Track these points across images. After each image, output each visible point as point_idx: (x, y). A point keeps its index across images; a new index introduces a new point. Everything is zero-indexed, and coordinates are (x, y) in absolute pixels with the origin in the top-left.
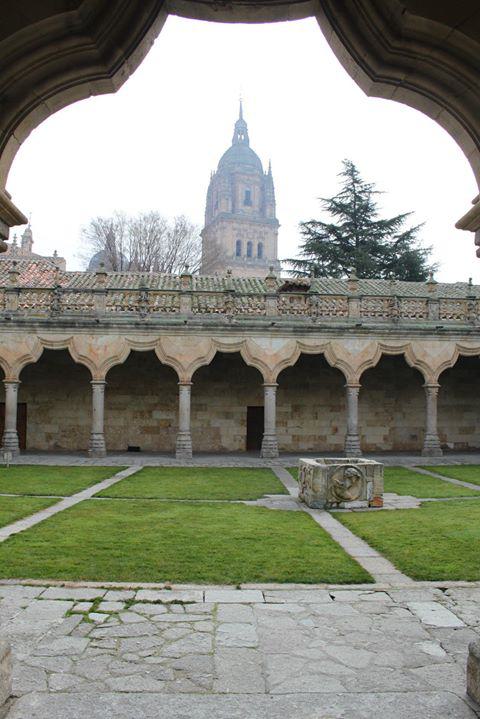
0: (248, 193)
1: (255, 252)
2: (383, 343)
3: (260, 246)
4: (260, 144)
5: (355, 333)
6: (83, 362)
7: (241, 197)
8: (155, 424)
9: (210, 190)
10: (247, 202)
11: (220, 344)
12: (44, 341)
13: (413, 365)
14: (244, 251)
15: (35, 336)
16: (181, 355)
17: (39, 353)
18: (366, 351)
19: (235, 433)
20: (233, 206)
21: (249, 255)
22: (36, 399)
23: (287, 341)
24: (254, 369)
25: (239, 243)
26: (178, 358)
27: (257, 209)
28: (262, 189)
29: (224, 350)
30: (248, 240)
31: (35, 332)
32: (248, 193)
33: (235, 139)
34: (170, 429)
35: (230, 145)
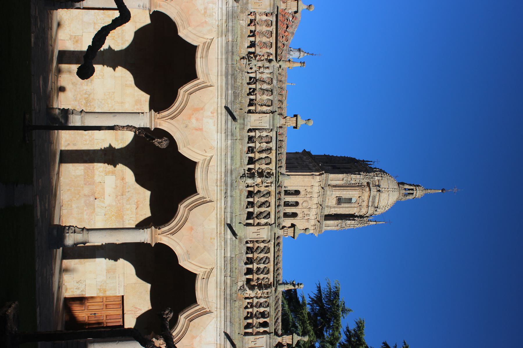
7: (345, 194)
8: (97, 179)
12: (208, 46)
15: (214, 35)
19: (88, 282)
21: (287, 204)
25: (297, 193)
27: (333, 211)
29: (199, 284)
31: (221, 34)
32: (349, 201)
34: (92, 199)
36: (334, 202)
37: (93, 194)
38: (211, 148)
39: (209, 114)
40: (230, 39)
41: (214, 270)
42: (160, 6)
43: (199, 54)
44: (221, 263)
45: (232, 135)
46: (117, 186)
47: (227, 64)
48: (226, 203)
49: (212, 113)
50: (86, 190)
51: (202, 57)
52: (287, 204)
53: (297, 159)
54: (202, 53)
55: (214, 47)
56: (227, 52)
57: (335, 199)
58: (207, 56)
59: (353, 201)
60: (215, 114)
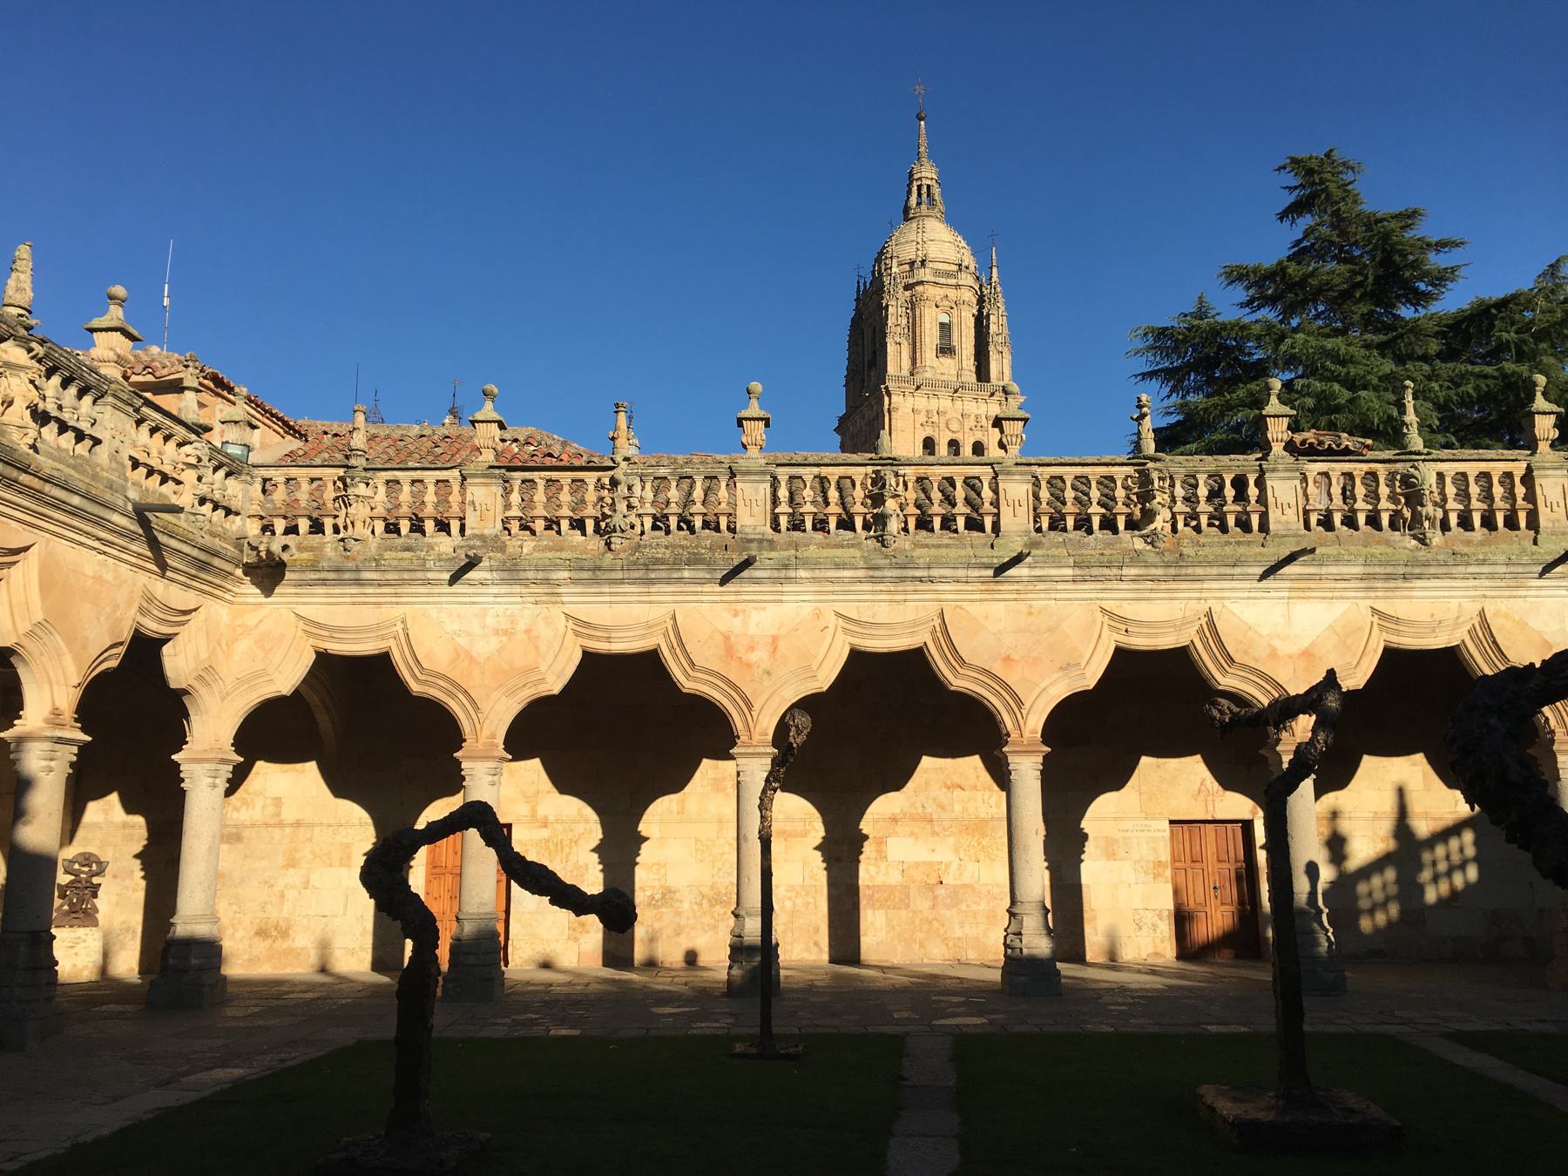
7: (931, 337)
8: (895, 878)
15: (556, 612)
16: (1007, 659)
19: (1137, 904)
22: (540, 812)
23: (1340, 607)
27: (969, 363)
30: (950, 436)
32: (945, 329)
34: (941, 891)
36: (948, 363)
37: (931, 888)
39: (738, 621)
40: (566, 574)
41: (1107, 605)
42: (493, 736)
44: (1088, 590)
45: (786, 567)
46: (912, 834)
47: (621, 581)
48: (943, 580)
49: (736, 615)
50: (922, 904)
51: (608, 640)
54: (598, 639)
55: (584, 612)
56: (595, 581)
58: (605, 628)
59: (945, 319)
60: (739, 606)
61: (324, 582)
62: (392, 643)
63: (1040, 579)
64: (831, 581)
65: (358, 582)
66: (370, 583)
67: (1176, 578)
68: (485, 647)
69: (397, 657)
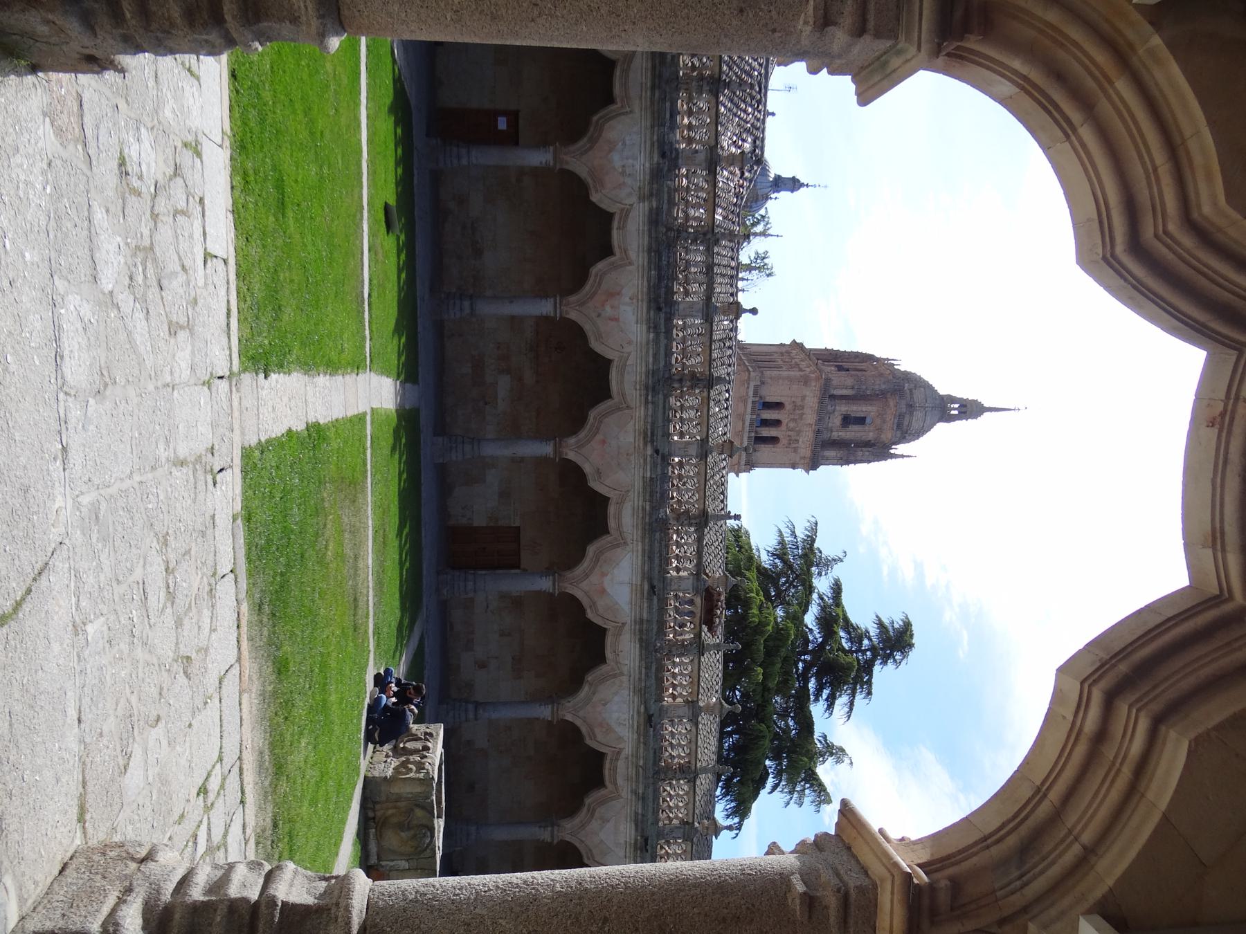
0: (861, 421)
1: (766, 432)
2: (623, 755)
3: (774, 440)
4: (942, 437)
5: (639, 712)
6: (591, 280)
7: (856, 409)
9: (870, 358)
10: (847, 420)
11: (621, 503)
12: (626, 213)
13: (588, 801)
14: (767, 415)
15: (634, 199)
17: (605, 205)
18: (609, 730)
20: (842, 397)
21: (765, 423)
23: (627, 608)
24: (581, 556)
25: (778, 406)
26: (599, 437)
27: (835, 435)
28: (867, 444)
30: (785, 422)
31: (642, 198)
32: (861, 421)
33: (952, 399)
35: (942, 390)
36: (837, 421)
38: (630, 343)
39: (627, 299)
40: (654, 205)
42: (567, 163)
43: (615, 224)
44: (638, 484)
45: (655, 327)
47: (650, 236)
51: (619, 228)
52: (765, 423)
53: (782, 354)
57: (840, 418)
59: (868, 421)
61: (654, 67)
62: (619, 105)
63: (645, 460)
64: (647, 352)
65: (653, 88)
66: (653, 95)
67: (644, 529)
68: (617, 159)
69: (613, 107)
